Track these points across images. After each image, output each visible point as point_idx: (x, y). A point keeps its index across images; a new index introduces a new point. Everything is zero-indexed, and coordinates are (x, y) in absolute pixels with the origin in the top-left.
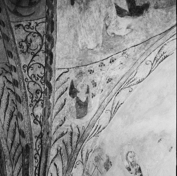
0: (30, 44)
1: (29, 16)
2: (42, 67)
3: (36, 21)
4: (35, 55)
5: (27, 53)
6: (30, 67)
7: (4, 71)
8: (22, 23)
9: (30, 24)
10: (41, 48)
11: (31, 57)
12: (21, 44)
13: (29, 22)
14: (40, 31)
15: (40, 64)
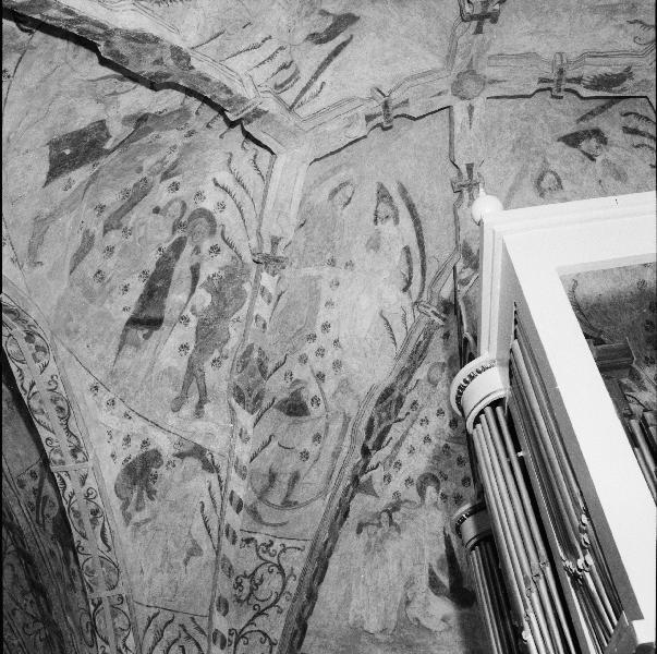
0: (257, 585)
1: (275, 525)
2: (267, 643)
3: (283, 541)
4: (260, 613)
5: (245, 603)
6: (243, 637)
7: (184, 635)
8: (257, 537)
9: (272, 543)
10: (276, 601)
11: (251, 613)
12: (239, 580)
13: (272, 538)
14: (284, 565)
15: (265, 634)
